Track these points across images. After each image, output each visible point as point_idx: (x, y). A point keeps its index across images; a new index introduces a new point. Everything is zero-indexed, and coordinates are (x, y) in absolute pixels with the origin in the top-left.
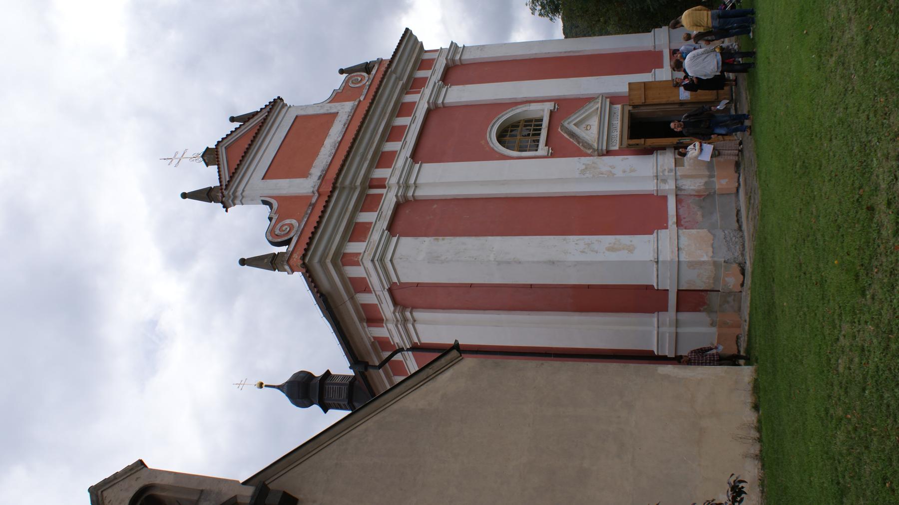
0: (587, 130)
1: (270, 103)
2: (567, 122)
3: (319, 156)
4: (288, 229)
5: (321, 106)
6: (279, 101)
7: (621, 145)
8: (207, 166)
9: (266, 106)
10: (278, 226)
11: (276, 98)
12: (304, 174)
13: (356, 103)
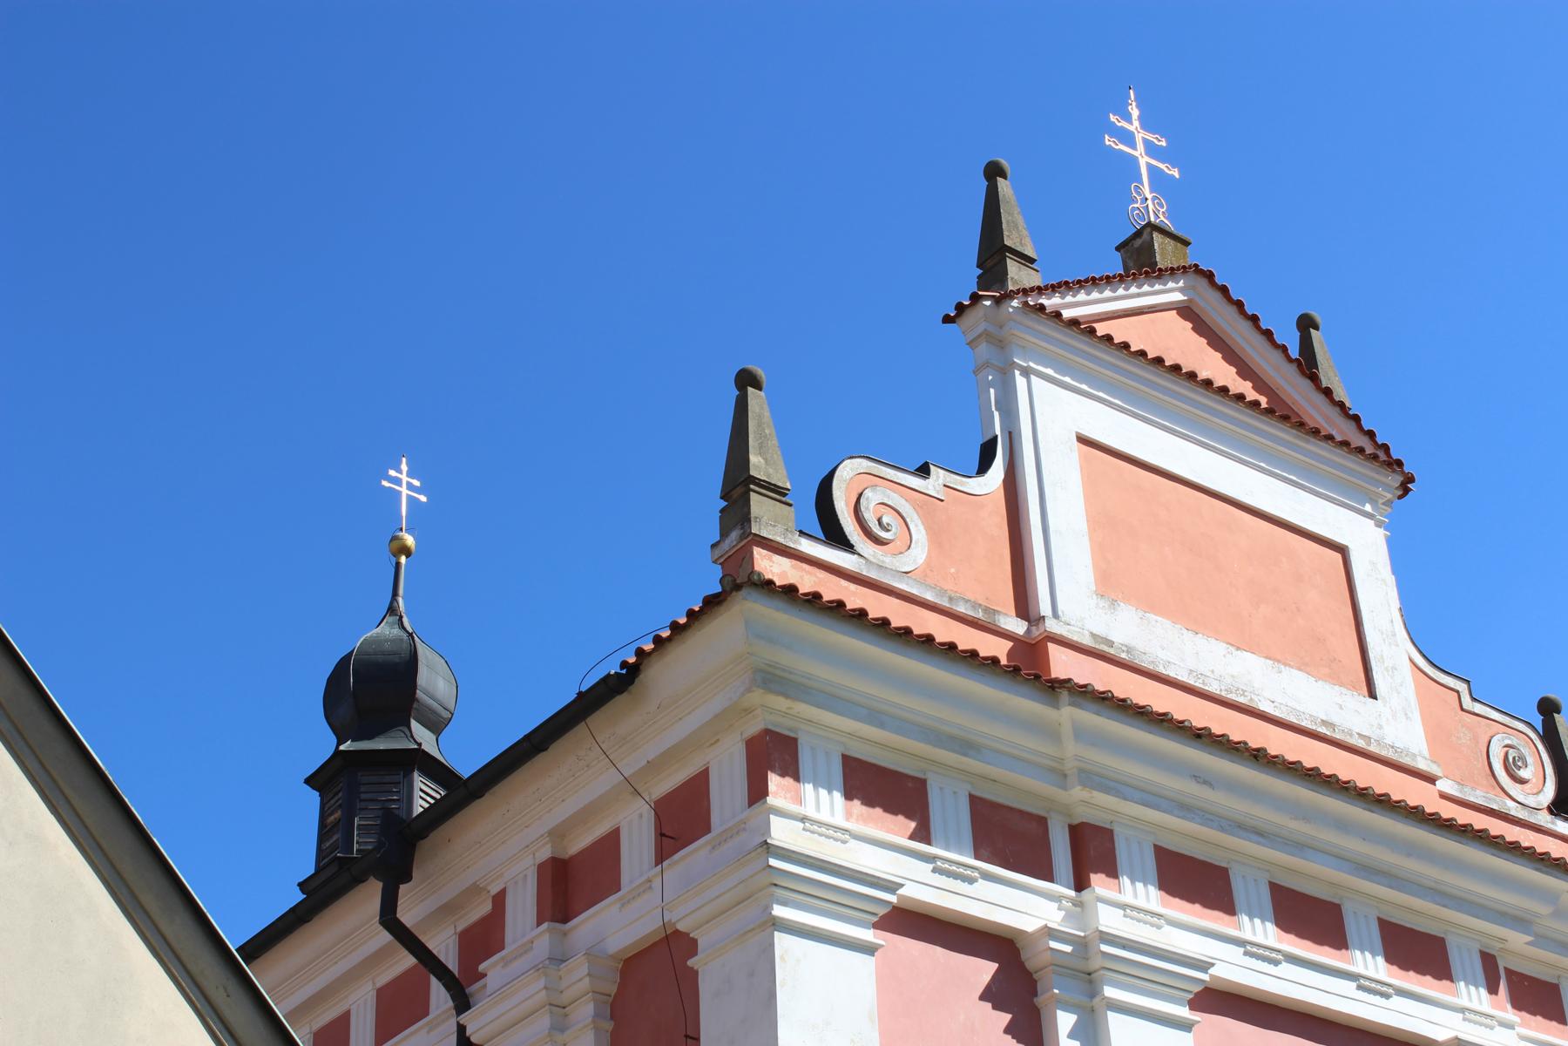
1: (1386, 448)
3: (1188, 635)
5: (1394, 635)
6: (1398, 479)
8: (1118, 249)
9: (1371, 435)
10: (895, 499)
11: (1406, 469)
12: (1110, 585)
13: (1422, 765)
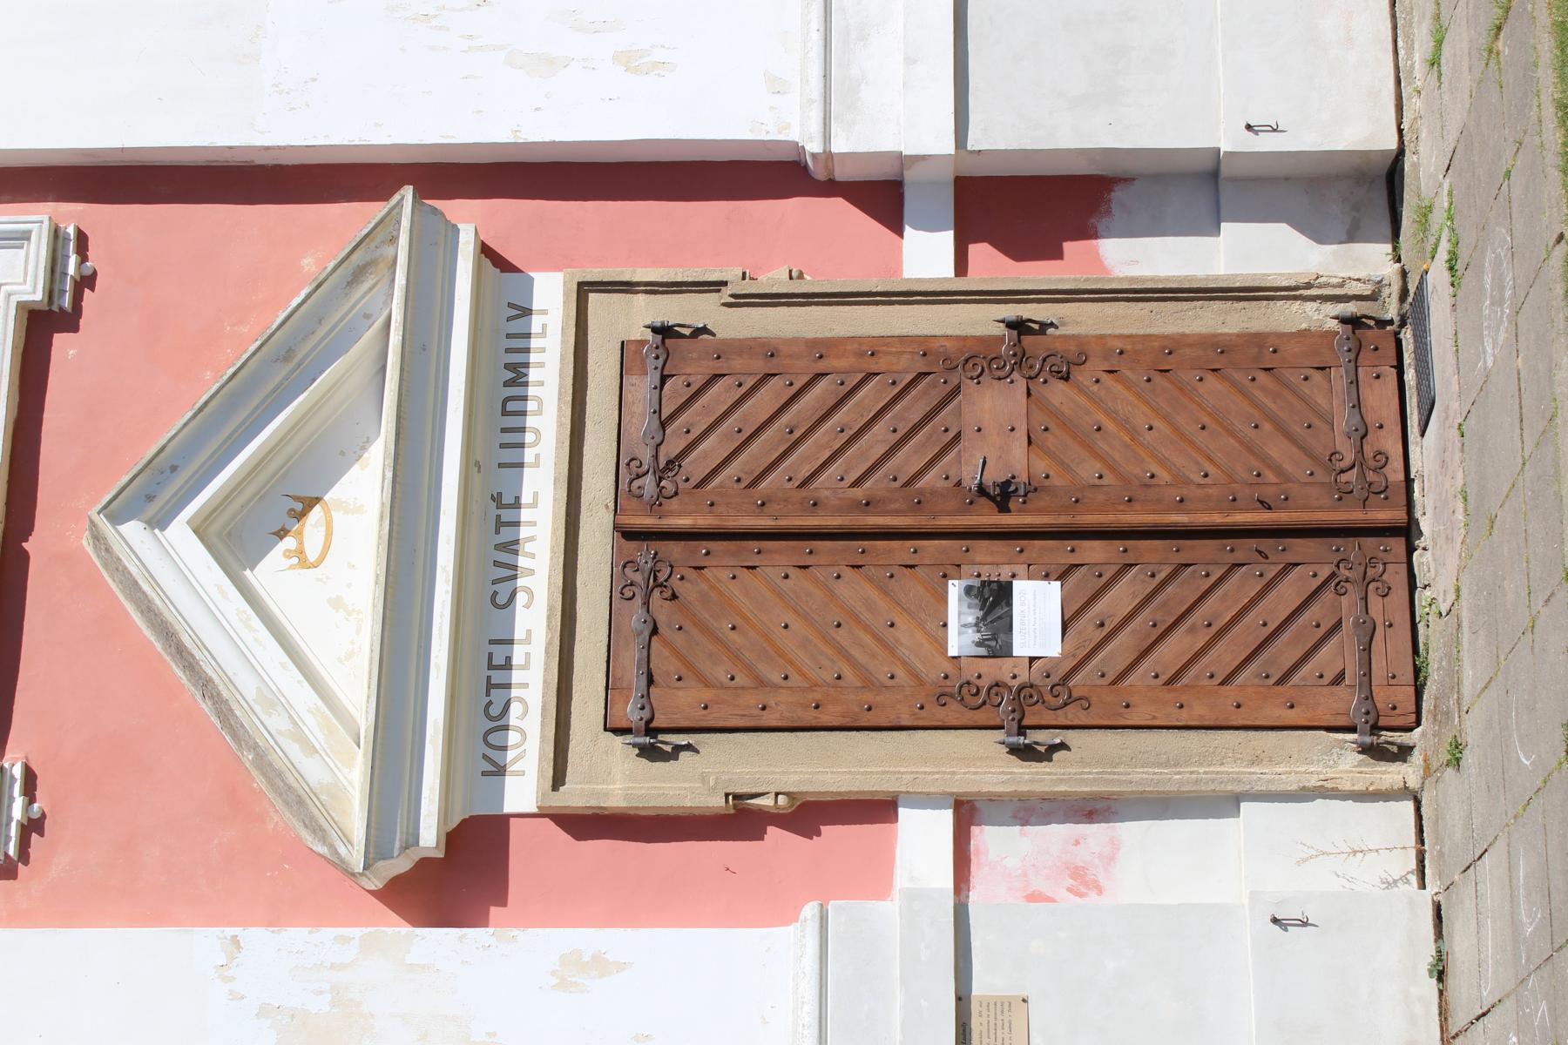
0: (304, 563)
7: (558, 780)
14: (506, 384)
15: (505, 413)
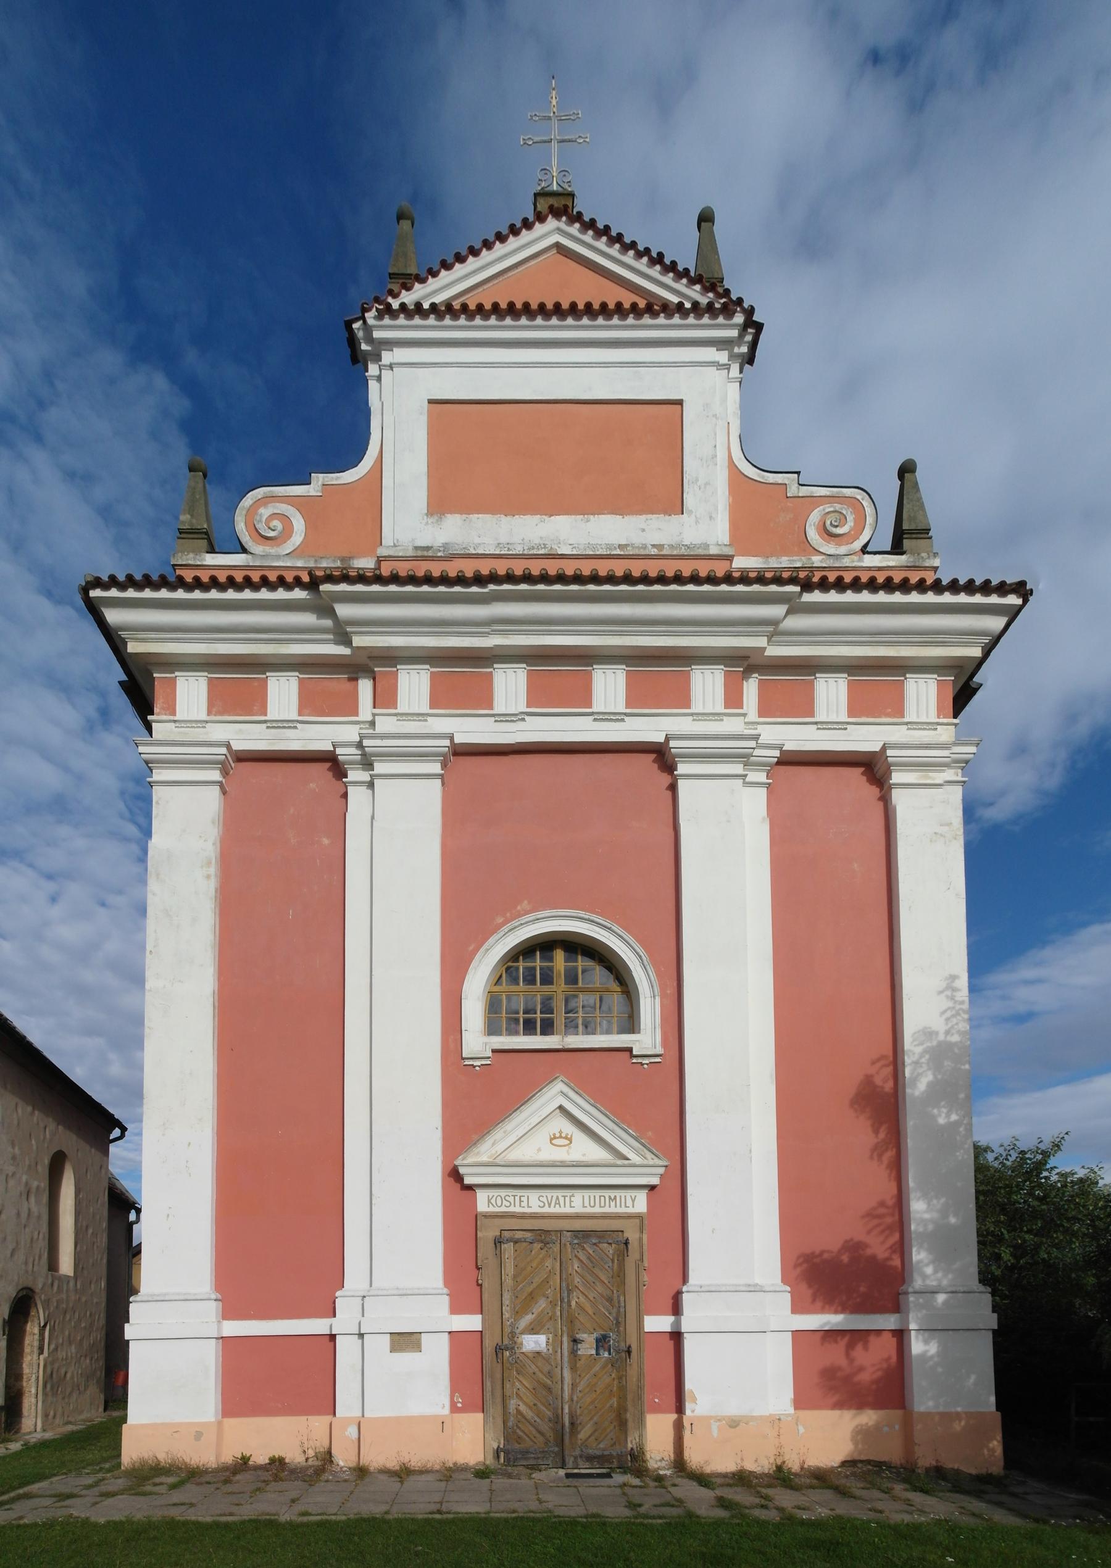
0: (551, 1139)
2: (566, 1089)
4: (272, 534)
14: (610, 1197)
15: (600, 1196)
